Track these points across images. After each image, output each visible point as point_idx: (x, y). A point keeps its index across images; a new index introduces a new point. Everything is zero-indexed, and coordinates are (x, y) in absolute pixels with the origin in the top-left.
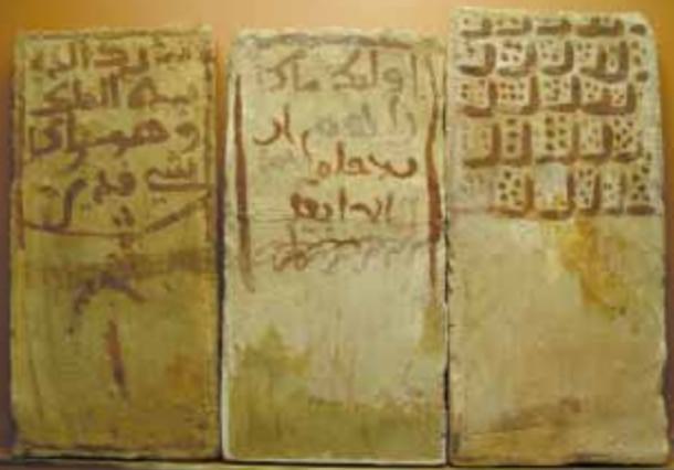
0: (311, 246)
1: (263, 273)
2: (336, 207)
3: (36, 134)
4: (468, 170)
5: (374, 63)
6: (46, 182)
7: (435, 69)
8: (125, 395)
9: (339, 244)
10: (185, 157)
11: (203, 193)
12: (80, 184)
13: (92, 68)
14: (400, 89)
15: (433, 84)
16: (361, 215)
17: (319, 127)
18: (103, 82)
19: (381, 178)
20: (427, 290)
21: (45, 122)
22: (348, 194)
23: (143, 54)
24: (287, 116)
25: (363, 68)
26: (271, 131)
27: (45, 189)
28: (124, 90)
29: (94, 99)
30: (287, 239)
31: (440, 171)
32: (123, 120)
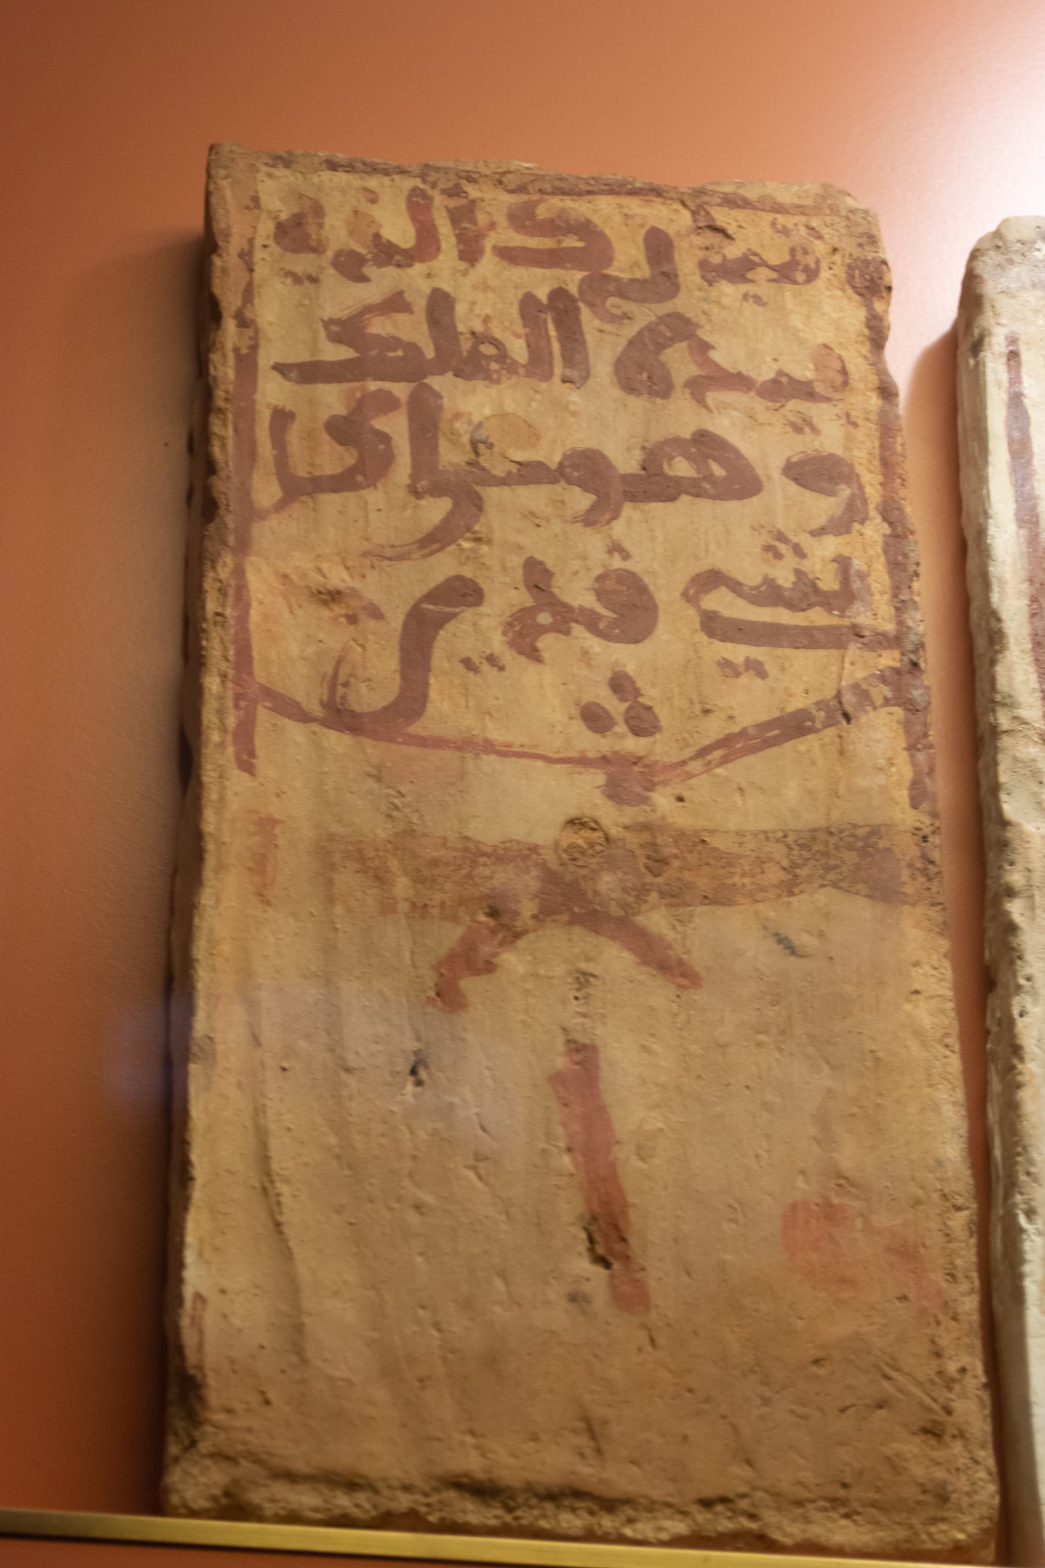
3: (294, 437)
6: (338, 578)
8: (632, 1298)
10: (831, 545)
11: (889, 659)
12: (463, 593)
13: (488, 264)
18: (529, 306)
21: (332, 399)
23: (659, 247)
27: (332, 597)
28: (604, 344)
29: (503, 356)
32: (608, 423)
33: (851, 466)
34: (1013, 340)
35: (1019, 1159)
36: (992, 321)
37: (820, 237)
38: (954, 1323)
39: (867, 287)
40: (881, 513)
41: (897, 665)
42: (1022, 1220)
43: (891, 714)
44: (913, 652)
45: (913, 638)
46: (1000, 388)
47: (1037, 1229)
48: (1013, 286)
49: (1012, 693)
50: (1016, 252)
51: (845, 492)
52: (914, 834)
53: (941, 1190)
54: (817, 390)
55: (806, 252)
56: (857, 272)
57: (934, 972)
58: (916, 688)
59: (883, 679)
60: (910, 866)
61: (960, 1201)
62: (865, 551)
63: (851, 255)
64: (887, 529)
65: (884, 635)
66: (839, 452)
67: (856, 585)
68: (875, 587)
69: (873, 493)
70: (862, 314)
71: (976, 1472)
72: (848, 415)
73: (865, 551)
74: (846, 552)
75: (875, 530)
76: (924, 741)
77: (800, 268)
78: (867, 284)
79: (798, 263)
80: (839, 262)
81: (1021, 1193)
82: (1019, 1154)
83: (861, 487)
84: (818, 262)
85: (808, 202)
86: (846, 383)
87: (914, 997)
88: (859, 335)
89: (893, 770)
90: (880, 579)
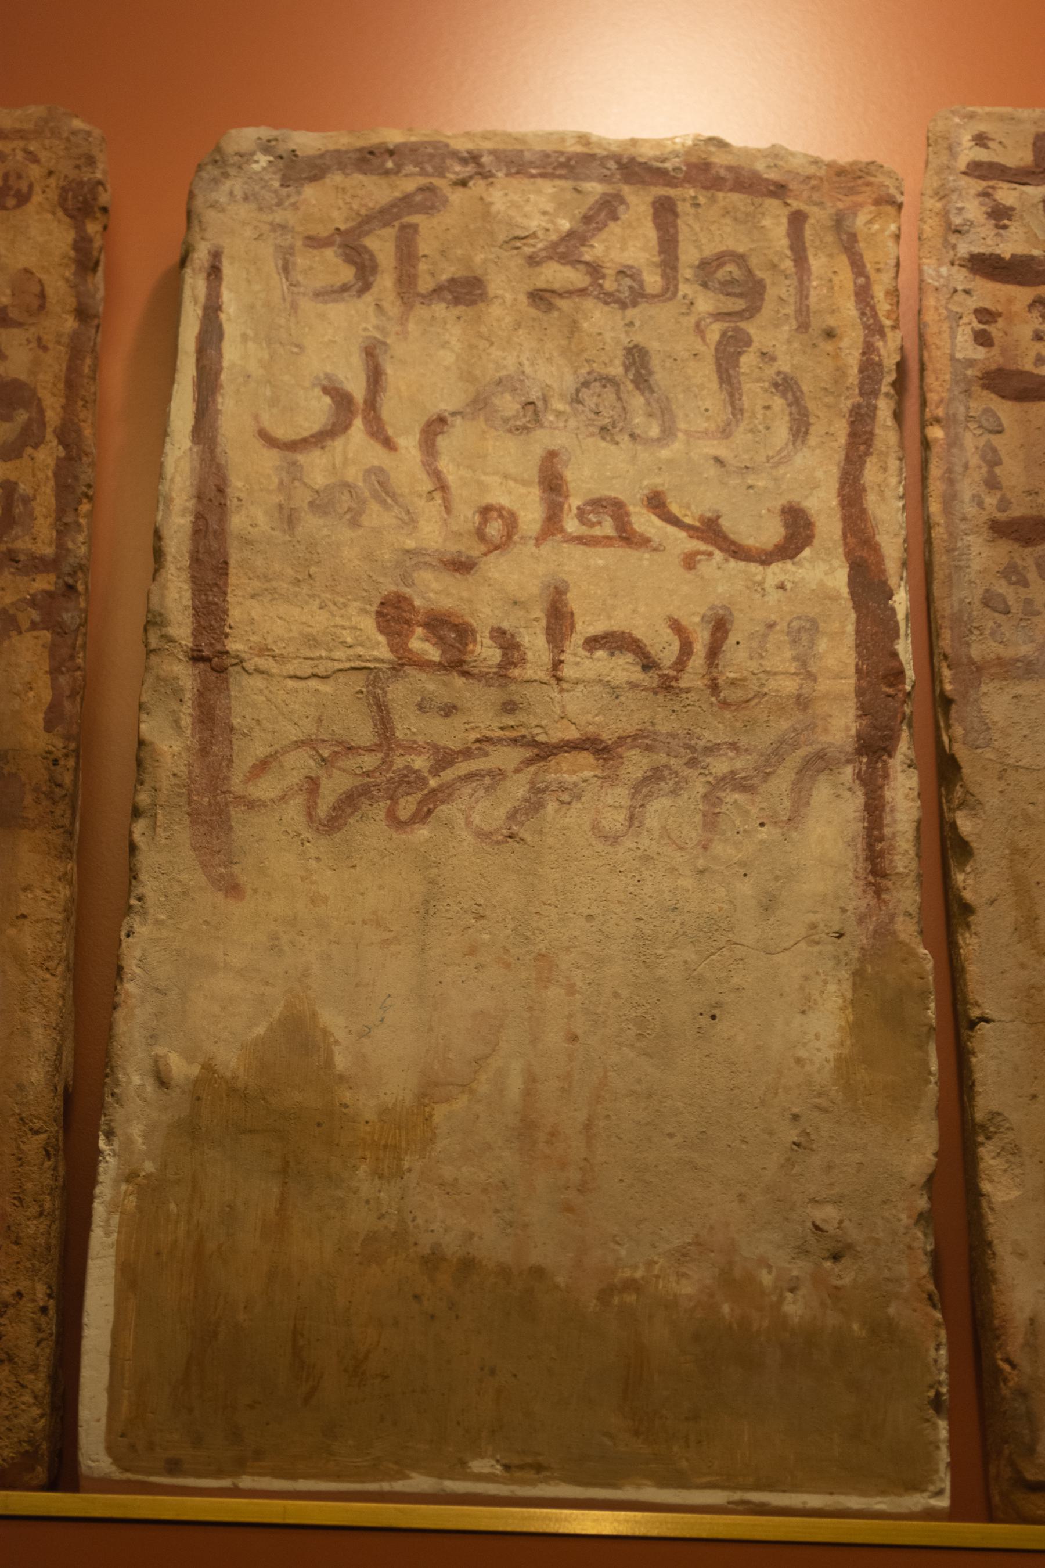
0: (444, 759)
1: (275, 841)
2: (535, 643)
4: (1003, 551)
5: (668, 244)
7: (869, 258)
9: (544, 752)
11: (44, 583)
14: (751, 312)
15: (863, 295)
16: (621, 668)
17: (479, 405)
19: (690, 561)
20: (857, 899)
22: (574, 601)
24: (375, 377)
25: (629, 244)
26: (316, 412)
30: (365, 734)
31: (891, 547)
33: (34, 391)
34: (216, 255)
35: (107, 1080)
36: (198, 236)
37: (36, 160)
38: (15, 1247)
39: (79, 209)
40: (58, 437)
41: (52, 588)
42: (102, 1143)
43: (37, 638)
44: (69, 574)
45: (71, 560)
46: (196, 303)
47: (113, 1150)
48: (223, 199)
49: (163, 611)
50: (233, 165)
51: (22, 416)
52: (44, 758)
53: (19, 1115)
54: (11, 315)
55: (19, 177)
56: (70, 194)
57: (46, 896)
58: (67, 610)
59: (33, 603)
60: (36, 790)
61: (37, 1124)
62: (34, 475)
63: (66, 177)
64: (61, 452)
65: (42, 559)
66: (23, 377)
67: (19, 509)
68: (39, 511)
69: (53, 416)
70: (70, 236)
71: (21, 1395)
72: (39, 339)
73: (34, 475)
74: (13, 478)
75: (47, 455)
76: (69, 664)
77: (12, 193)
78: (80, 205)
79: (10, 188)
80: (53, 185)
81: (105, 1115)
82: (107, 1076)
83: (41, 411)
84: (31, 186)
85: (30, 126)
86: (42, 307)
87: (20, 922)
88: (64, 258)
89: (31, 694)
90: (45, 502)
